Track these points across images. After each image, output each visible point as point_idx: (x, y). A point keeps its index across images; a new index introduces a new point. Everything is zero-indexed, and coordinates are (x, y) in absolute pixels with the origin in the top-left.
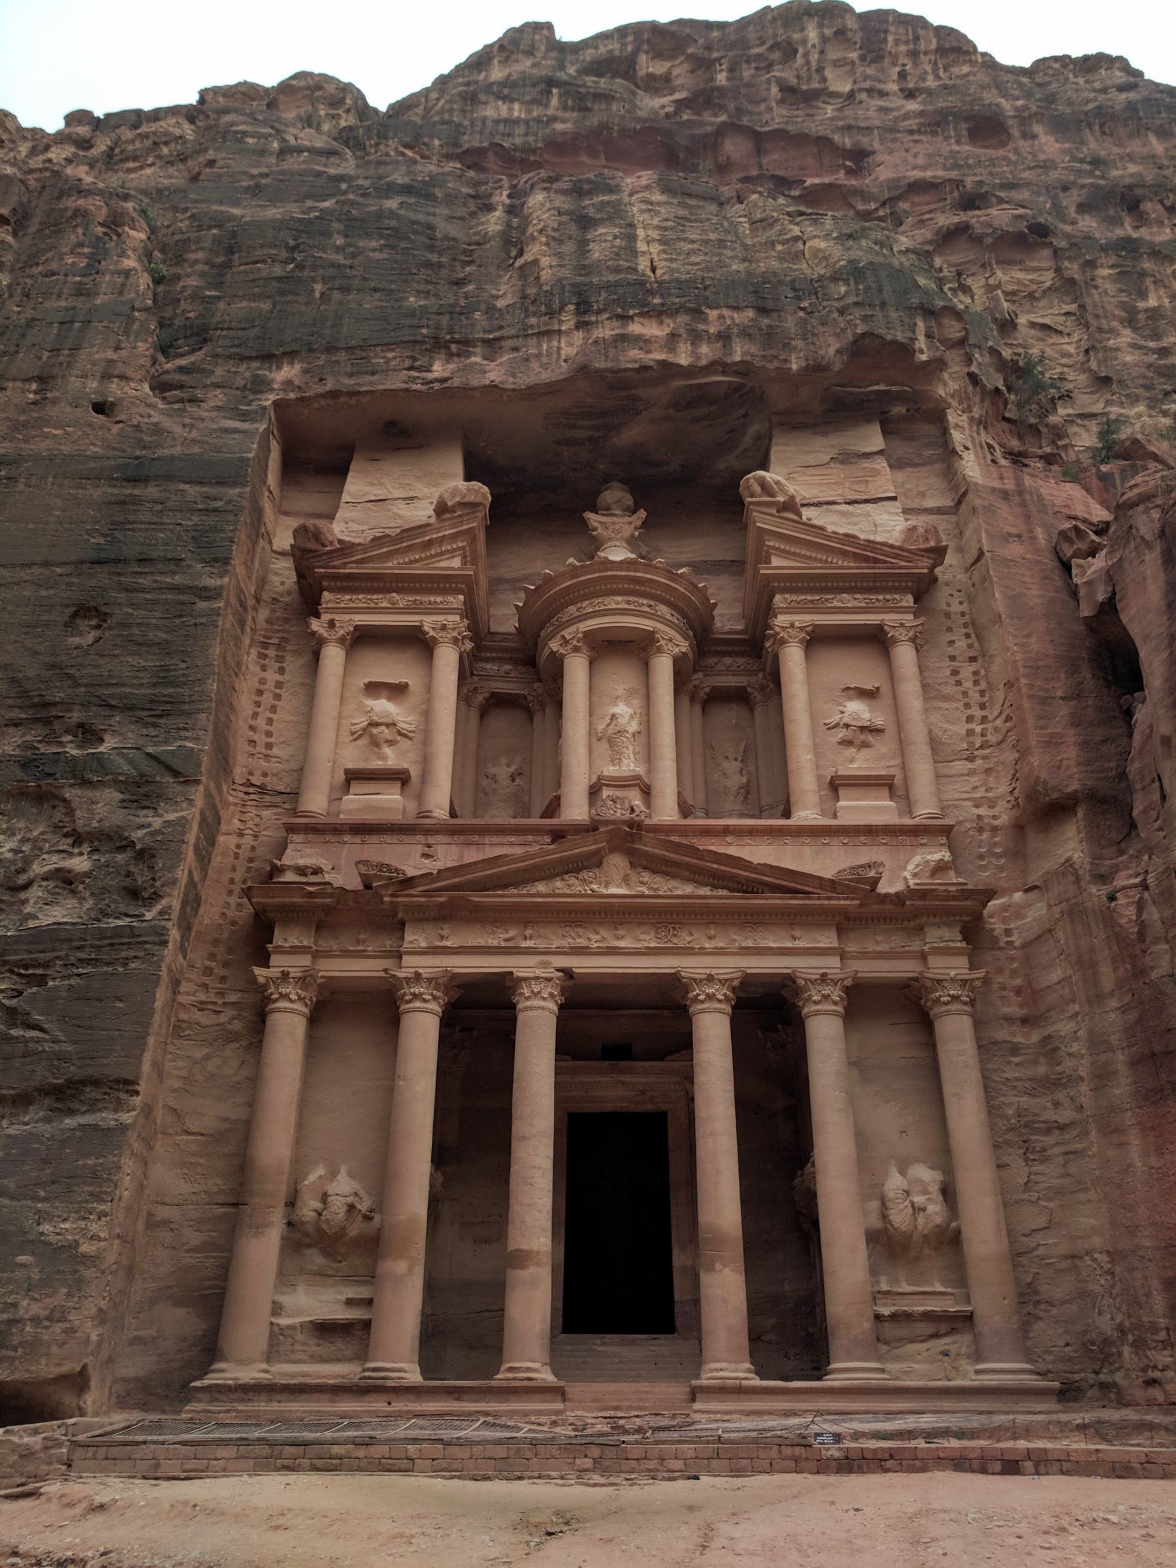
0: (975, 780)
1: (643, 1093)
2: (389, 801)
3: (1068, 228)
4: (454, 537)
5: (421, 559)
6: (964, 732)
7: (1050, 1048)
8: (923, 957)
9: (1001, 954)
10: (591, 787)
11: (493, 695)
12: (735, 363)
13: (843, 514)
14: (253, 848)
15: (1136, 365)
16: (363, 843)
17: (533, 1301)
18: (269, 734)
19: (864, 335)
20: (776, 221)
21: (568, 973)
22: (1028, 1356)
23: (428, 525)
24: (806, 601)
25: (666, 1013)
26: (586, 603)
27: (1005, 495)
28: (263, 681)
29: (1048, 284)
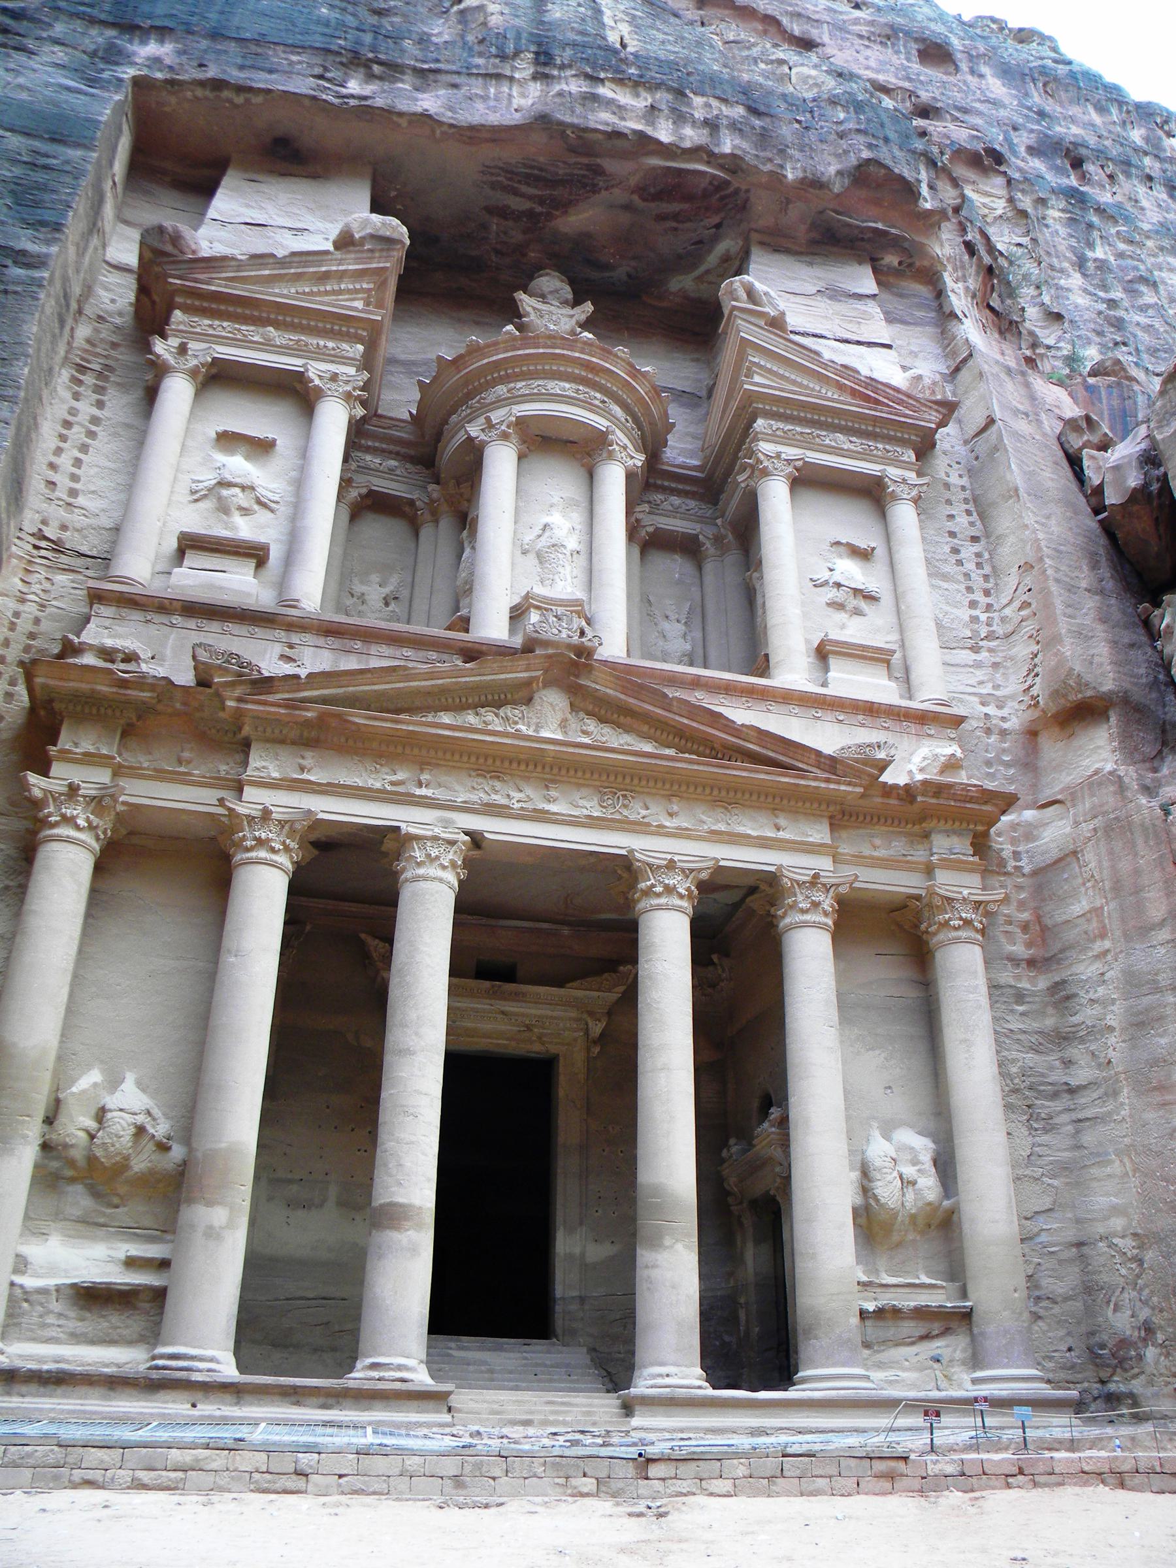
0: (980, 674)
1: (529, 1028)
2: (238, 583)
3: (1022, 164)
4: (360, 274)
5: (311, 293)
6: (968, 619)
7: (1062, 996)
8: (929, 870)
9: (1009, 882)
10: (513, 609)
11: (371, 493)
12: (724, 156)
13: (833, 350)
14: (37, 621)
15: (1087, 309)
16: (199, 629)
17: (405, 1276)
18: (75, 478)
19: (868, 161)
21: (476, 839)
23: (327, 252)
25: (566, 931)
26: (519, 385)
27: (1009, 371)
28: (73, 412)
29: (999, 212)
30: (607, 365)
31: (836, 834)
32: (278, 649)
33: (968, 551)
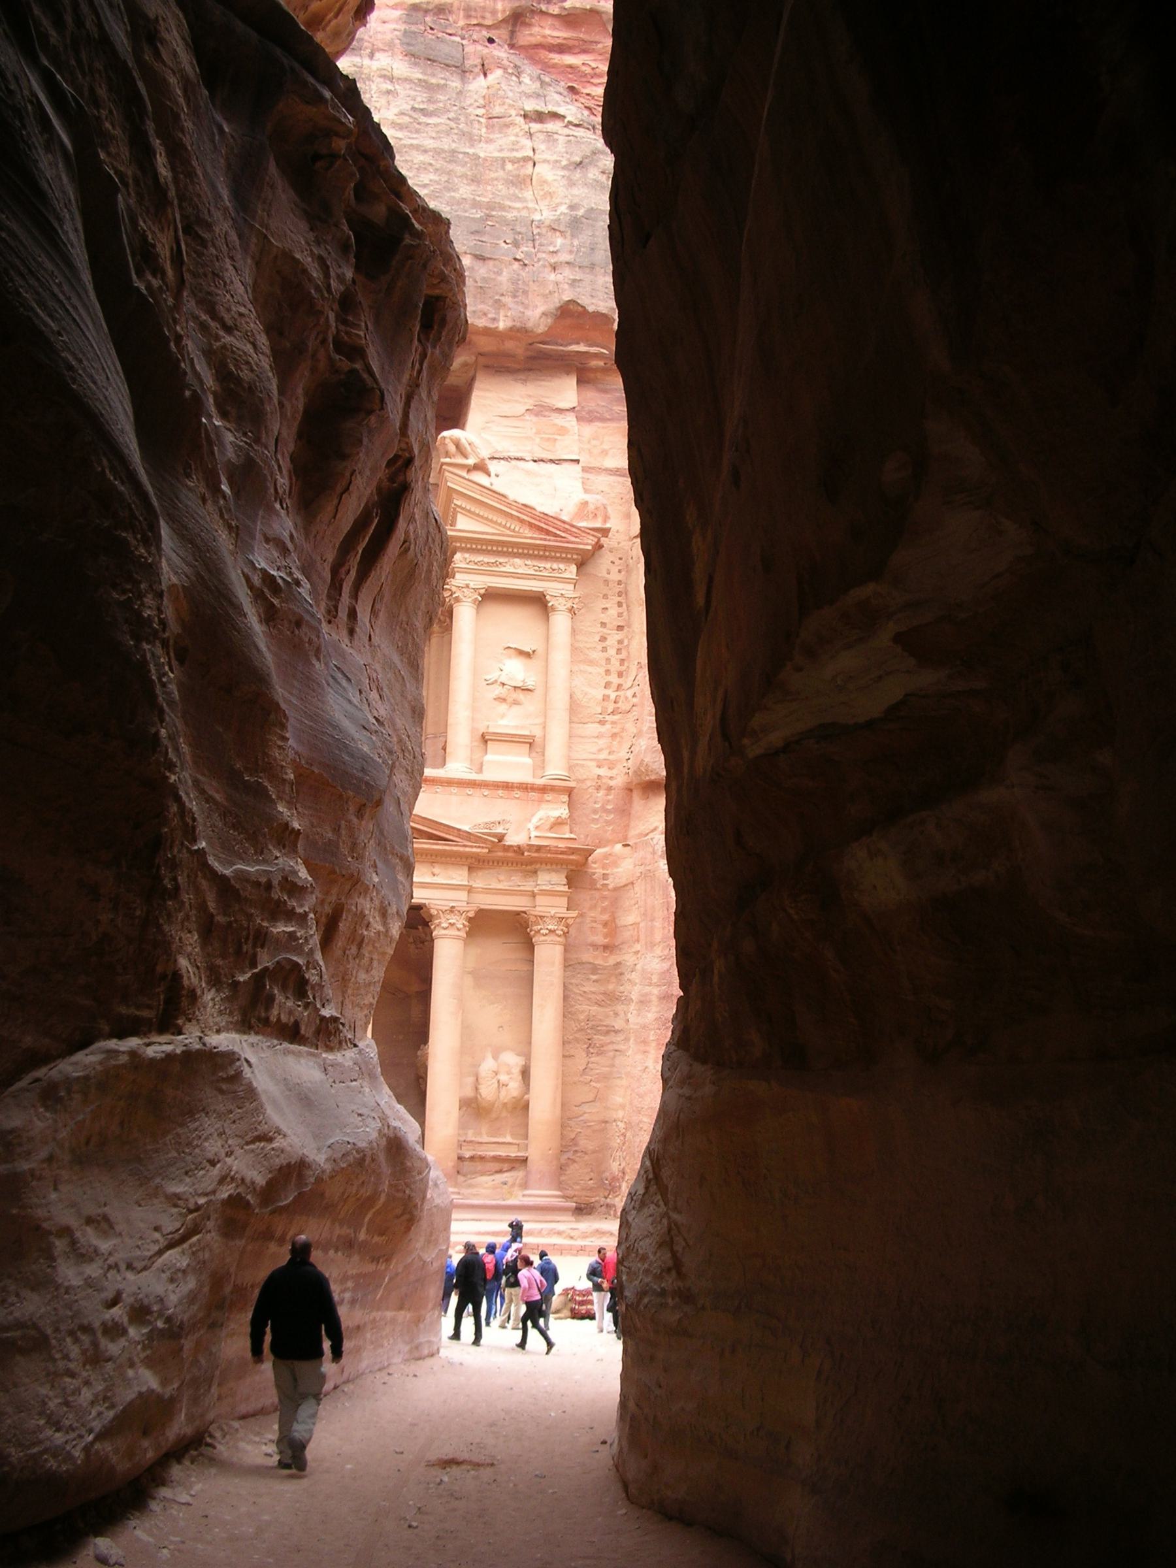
0: (602, 742)
6: (601, 697)
8: (533, 895)
9: (597, 894)
20: (512, 124)
22: (560, 1185)
33: (614, 638)
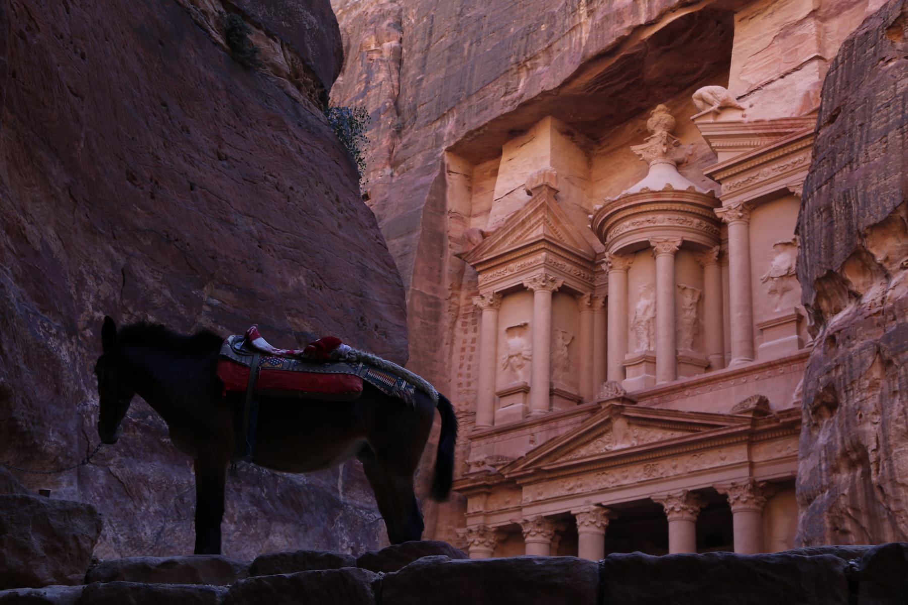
4: (536, 211)
5: (523, 234)
16: (503, 440)
21: (599, 505)
23: (518, 212)
24: (739, 184)
28: (464, 342)
30: (640, 201)
31: (757, 450)
32: (528, 438)
